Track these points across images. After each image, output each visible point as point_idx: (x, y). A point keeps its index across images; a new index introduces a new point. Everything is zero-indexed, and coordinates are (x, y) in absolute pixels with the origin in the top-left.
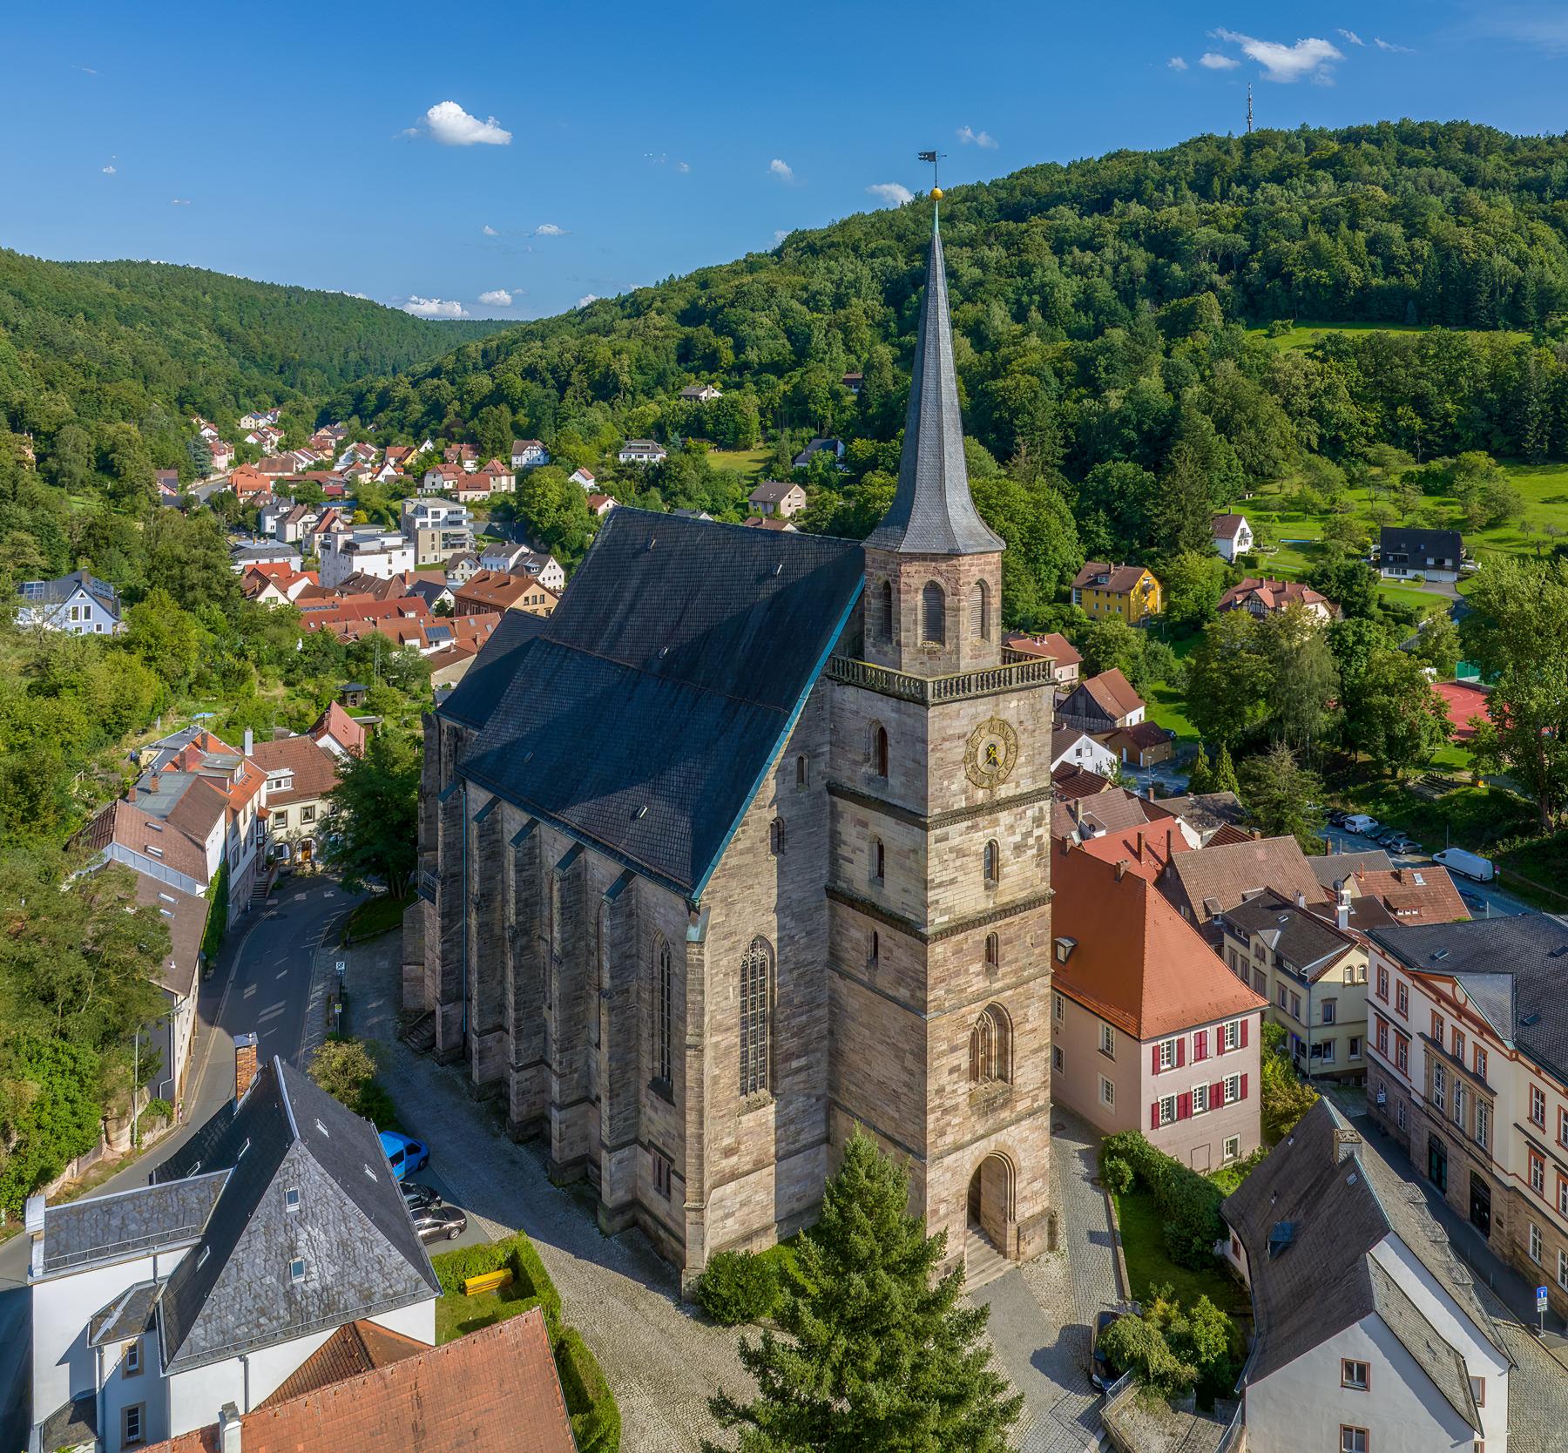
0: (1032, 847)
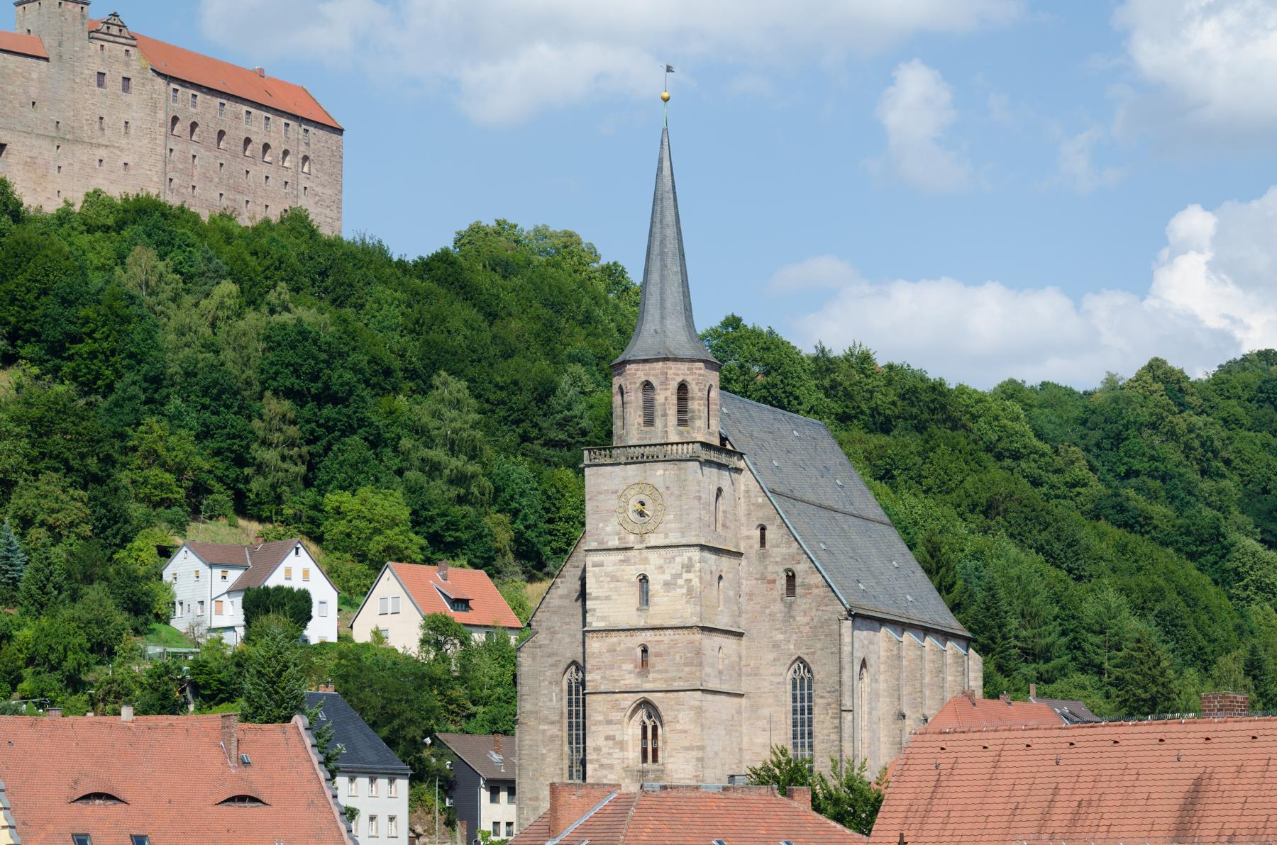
0: (681, 587)
